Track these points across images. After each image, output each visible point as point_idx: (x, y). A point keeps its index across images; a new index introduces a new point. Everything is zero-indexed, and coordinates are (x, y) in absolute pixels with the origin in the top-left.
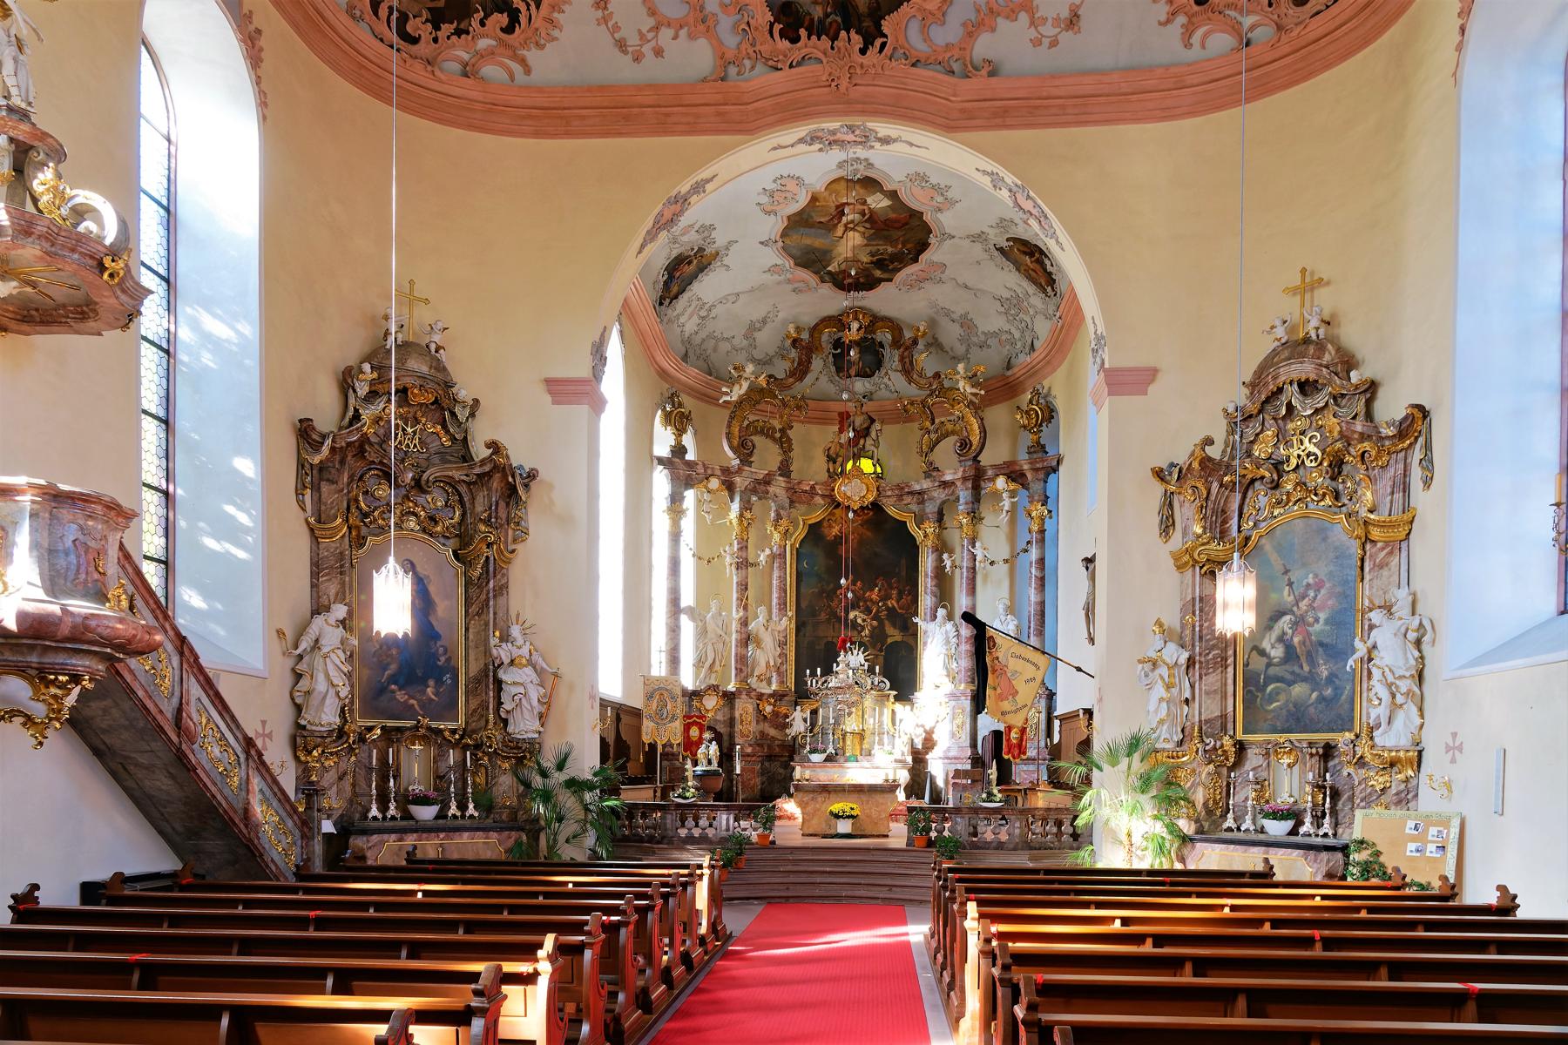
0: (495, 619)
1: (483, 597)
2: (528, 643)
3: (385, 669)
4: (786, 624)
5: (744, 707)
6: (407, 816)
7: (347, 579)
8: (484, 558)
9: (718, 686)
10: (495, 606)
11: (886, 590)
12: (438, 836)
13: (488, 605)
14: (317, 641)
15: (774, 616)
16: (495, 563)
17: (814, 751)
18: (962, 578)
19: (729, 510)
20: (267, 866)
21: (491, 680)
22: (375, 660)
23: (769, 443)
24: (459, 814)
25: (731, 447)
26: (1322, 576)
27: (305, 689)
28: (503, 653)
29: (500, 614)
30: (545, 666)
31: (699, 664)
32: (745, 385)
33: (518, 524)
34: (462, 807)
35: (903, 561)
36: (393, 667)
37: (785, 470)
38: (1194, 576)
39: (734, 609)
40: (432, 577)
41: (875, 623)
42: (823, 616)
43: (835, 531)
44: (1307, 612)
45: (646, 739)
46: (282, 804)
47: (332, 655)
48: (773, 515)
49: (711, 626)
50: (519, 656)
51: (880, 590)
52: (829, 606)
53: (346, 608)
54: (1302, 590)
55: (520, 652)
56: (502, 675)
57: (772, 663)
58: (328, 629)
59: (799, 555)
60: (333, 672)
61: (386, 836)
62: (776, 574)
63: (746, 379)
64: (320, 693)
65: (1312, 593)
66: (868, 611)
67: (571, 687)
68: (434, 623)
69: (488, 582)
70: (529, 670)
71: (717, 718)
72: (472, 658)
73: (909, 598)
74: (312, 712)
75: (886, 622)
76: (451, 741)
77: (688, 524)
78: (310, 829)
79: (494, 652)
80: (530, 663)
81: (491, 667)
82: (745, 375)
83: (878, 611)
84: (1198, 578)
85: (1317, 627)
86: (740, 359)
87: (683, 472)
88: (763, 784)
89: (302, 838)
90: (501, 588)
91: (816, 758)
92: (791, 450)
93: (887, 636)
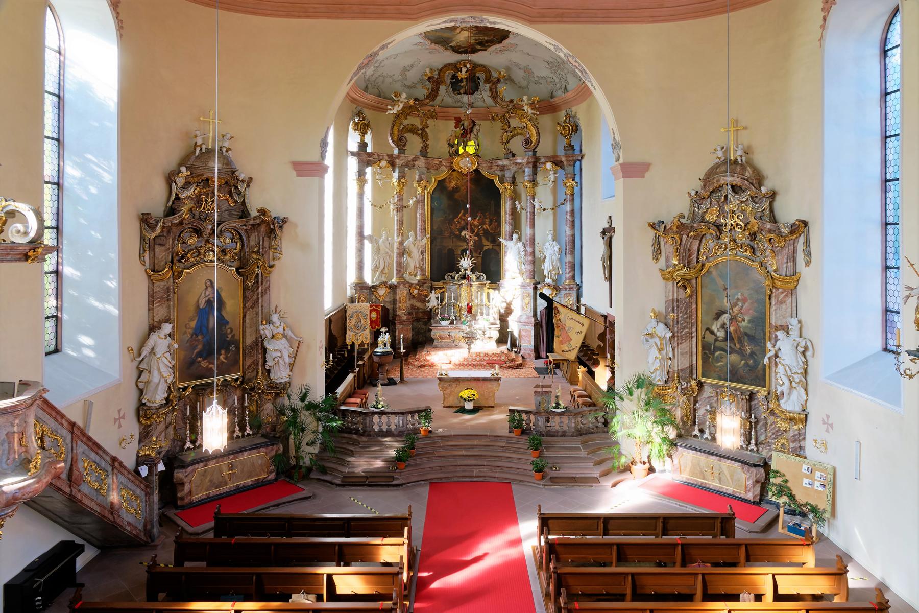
0: (262, 309)
1: (255, 297)
4: (426, 242)
5: (402, 293)
9: (386, 283)
10: (262, 302)
11: (482, 219)
13: (258, 302)
15: (418, 236)
17: (443, 319)
18: (527, 218)
19: (391, 177)
21: (260, 347)
23: (415, 136)
25: (393, 141)
26: (746, 295)
28: (267, 331)
29: (265, 305)
30: (293, 336)
31: (375, 269)
32: (401, 105)
35: (492, 202)
37: (424, 152)
38: (673, 286)
39: (395, 235)
41: (476, 238)
42: (446, 234)
43: (453, 184)
44: (737, 314)
45: (349, 342)
48: (417, 177)
49: (382, 247)
50: (278, 333)
51: (479, 220)
52: (451, 228)
54: (735, 301)
55: (278, 330)
56: (266, 345)
57: (418, 266)
59: (432, 198)
62: (419, 211)
63: (402, 102)
65: (740, 304)
66: (472, 231)
69: (258, 288)
70: (284, 341)
71: (386, 300)
73: (496, 224)
75: (483, 238)
77: (368, 188)
79: (262, 332)
80: (284, 336)
82: (401, 100)
83: (478, 232)
84: (676, 289)
85: (744, 324)
86: (398, 86)
87: (365, 158)
88: (412, 335)
90: (266, 290)
91: (444, 323)
92: (427, 140)
93: (483, 246)
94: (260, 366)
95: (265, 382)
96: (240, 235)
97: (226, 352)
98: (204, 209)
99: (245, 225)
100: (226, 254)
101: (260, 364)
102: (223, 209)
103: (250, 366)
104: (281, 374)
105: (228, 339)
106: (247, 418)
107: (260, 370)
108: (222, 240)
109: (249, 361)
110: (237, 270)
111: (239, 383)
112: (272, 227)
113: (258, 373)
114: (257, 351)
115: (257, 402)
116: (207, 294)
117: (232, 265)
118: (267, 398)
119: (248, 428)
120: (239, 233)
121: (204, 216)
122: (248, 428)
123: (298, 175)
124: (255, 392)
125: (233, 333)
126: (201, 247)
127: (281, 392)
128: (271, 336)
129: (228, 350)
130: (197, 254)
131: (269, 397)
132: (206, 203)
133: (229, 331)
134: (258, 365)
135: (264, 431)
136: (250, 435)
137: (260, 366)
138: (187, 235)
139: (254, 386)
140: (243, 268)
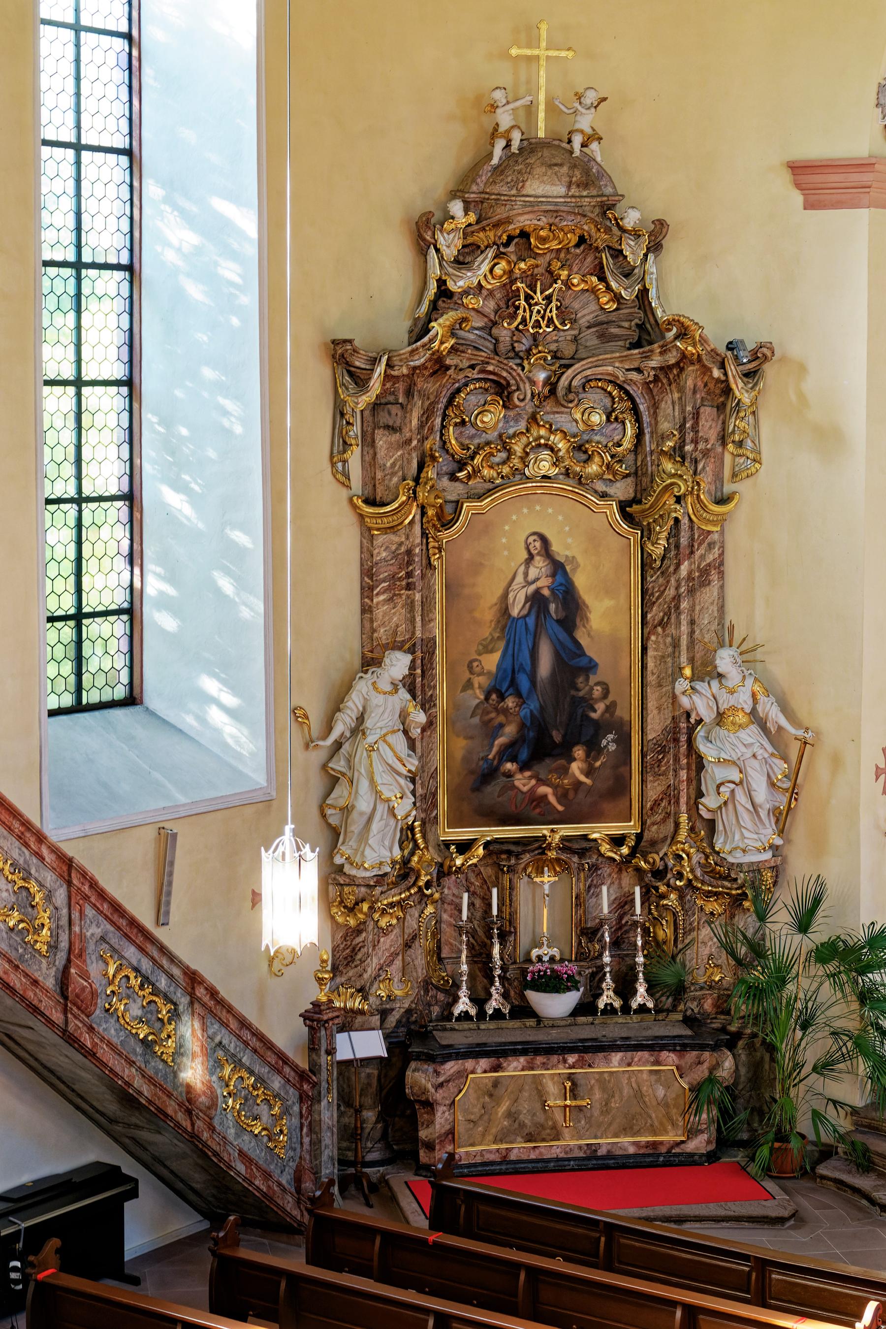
0: (692, 632)
1: (671, 592)
2: (749, 681)
3: (494, 737)
6: (523, 1011)
7: (418, 597)
8: (672, 522)
10: (692, 609)
12: (565, 1061)
13: (677, 607)
14: (361, 719)
16: (691, 528)
20: (230, 1167)
21: (684, 748)
22: (476, 720)
24: (617, 1004)
27: (342, 803)
30: (783, 721)
33: (740, 444)
34: (625, 990)
36: (510, 731)
40: (580, 559)
46: (262, 1057)
47: (383, 747)
50: (734, 708)
53: (409, 657)
58: (377, 700)
60: (382, 778)
61: (469, 1064)
64: (362, 814)
67: (836, 761)
68: (584, 641)
70: (751, 735)
72: (651, 704)
74: (353, 843)
76: (614, 860)
78: (315, 1085)
81: (683, 725)
89: (301, 1100)
90: (705, 572)
94: (683, 808)
95: (697, 857)
96: (631, 398)
97: (588, 755)
98: (524, 321)
99: (639, 370)
100: (589, 459)
101: (683, 800)
102: (583, 322)
103: (656, 803)
104: (743, 837)
105: (594, 715)
106: (640, 959)
107: (684, 818)
108: (578, 416)
109: (654, 791)
110: (623, 507)
111: (625, 850)
112: (716, 373)
113: (677, 825)
114: (677, 760)
115: (675, 915)
116: (531, 576)
117: (611, 491)
118: (708, 908)
119: (641, 989)
120: (627, 393)
121: (526, 343)
122: (641, 989)
123: (809, 205)
124: (668, 885)
125: (611, 698)
126: (514, 435)
127: (744, 894)
128: (714, 715)
129: (593, 748)
130: (504, 455)
131: (714, 906)
132: (530, 305)
133: (598, 691)
134: (677, 802)
135: (693, 1005)
136: (649, 1010)
137: (683, 808)
138: (473, 399)
139: (666, 866)
140: (639, 502)
